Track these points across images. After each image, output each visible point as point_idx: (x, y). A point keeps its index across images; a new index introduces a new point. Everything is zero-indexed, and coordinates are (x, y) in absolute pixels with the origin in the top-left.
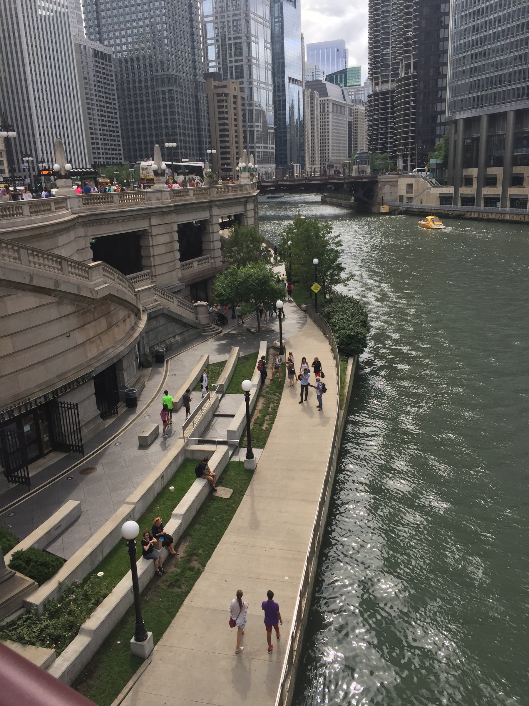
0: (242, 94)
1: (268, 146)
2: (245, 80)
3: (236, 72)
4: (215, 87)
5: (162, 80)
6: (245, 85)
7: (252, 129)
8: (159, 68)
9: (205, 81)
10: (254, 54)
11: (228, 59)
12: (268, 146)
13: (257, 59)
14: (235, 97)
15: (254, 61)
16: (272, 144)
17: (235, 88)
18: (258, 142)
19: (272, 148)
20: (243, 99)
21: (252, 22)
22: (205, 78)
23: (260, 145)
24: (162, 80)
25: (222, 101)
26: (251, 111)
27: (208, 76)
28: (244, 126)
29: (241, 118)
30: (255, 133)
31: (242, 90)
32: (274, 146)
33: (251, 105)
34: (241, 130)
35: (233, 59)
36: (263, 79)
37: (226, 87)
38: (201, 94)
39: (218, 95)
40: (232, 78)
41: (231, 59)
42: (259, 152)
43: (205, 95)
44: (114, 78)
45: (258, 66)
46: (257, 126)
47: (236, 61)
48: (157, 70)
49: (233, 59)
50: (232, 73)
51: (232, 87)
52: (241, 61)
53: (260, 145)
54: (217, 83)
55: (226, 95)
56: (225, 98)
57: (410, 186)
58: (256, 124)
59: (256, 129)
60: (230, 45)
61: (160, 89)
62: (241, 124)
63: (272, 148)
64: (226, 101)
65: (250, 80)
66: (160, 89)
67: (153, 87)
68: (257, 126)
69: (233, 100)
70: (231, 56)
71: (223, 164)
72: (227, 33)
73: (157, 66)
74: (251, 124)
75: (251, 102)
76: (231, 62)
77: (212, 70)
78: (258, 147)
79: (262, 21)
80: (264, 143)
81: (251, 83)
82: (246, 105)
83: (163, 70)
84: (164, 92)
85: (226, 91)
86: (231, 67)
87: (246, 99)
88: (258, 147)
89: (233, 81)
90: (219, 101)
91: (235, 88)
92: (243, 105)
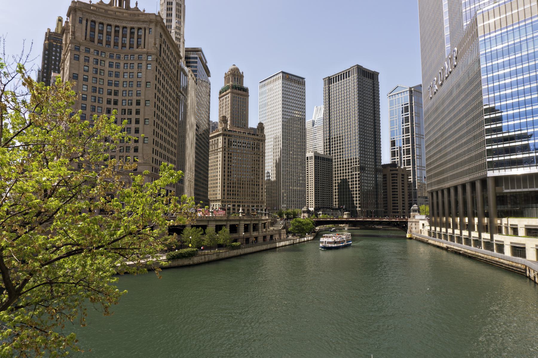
4: (391, 170)
5: (356, 169)
8: (355, 163)
11: (403, 157)
14: (403, 175)
24: (356, 169)
27: (385, 166)
35: (405, 156)
39: (392, 174)
55: (397, 174)
56: (396, 176)
57: (423, 225)
61: (354, 173)
66: (354, 173)
67: (351, 172)
69: (401, 176)
70: (404, 155)
71: (393, 209)
84: (356, 174)
90: (392, 177)
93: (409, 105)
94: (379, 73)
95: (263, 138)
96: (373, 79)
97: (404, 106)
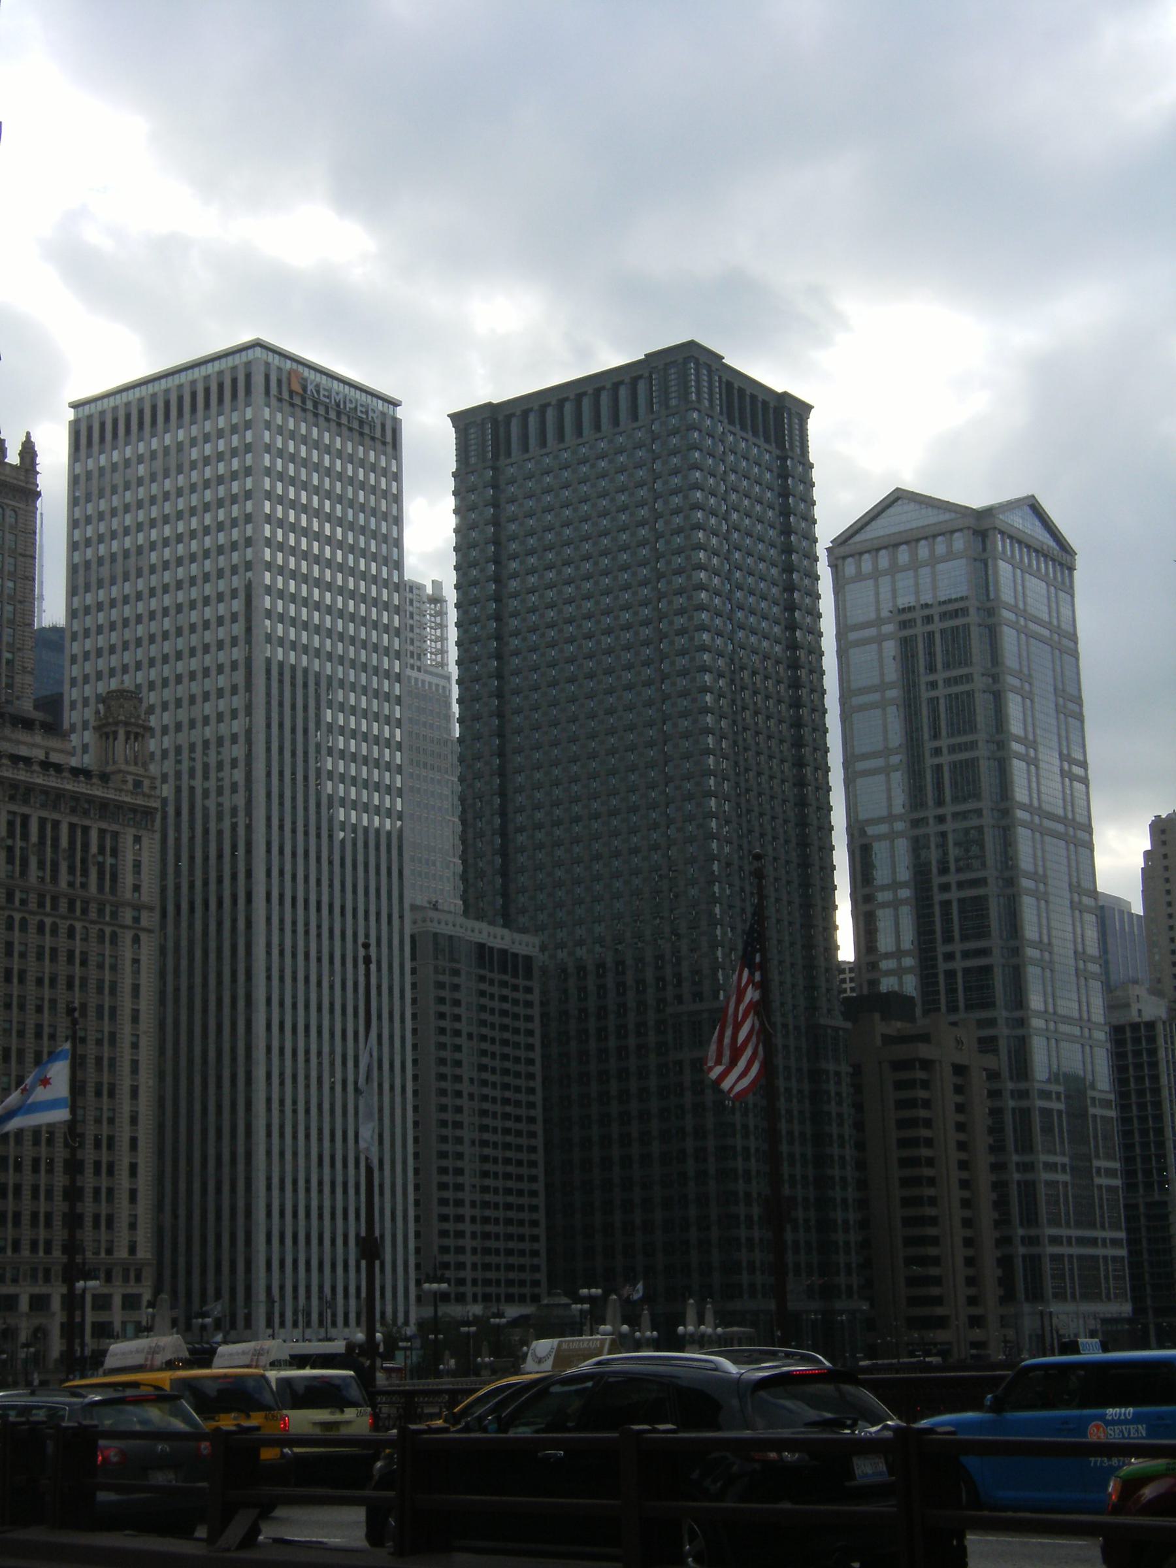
0: (990, 1061)
1: (1099, 1234)
2: (1002, 1013)
3: (965, 989)
4: (888, 1040)
6: (1003, 1031)
7: (1029, 1176)
9: (849, 1025)
10: (1030, 931)
12: (1099, 1234)
13: (1046, 946)
14: (960, 1070)
15: (1031, 953)
16: (1116, 1226)
17: (959, 1042)
18: (1055, 1222)
19: (1115, 1242)
20: (993, 1075)
21: (1023, 834)
22: (847, 1016)
23: (1064, 1232)
25: (911, 1084)
26: (1024, 1115)
28: (998, 1167)
29: (982, 1140)
30: (1042, 1191)
31: (988, 1045)
32: (1122, 1235)
33: (1023, 1094)
34: (984, 1179)
35: (957, 947)
36: (1068, 1006)
37: (925, 1038)
38: (831, 1067)
40: (953, 1008)
41: (949, 948)
42: (1056, 1258)
43: (845, 1068)
44: (536, 1026)
45: (1048, 966)
46: (1051, 1167)
47: (966, 955)
48: (679, 999)
49: (957, 947)
50: (955, 991)
51: (951, 1042)
52: (984, 952)
53: (1064, 1232)
54: (896, 1027)
55: (927, 1065)
56: (921, 1075)
58: (1043, 1158)
59: (1046, 1176)
60: (946, 904)
62: (983, 1159)
63: (1115, 1242)
64: (925, 1084)
65: (1017, 1014)
68: (1051, 1167)
72: (934, 870)
73: (679, 984)
74: (1027, 1158)
75: (1022, 1086)
76: (949, 957)
77: (887, 984)
78: (1055, 1240)
79: (1060, 828)
80: (1079, 1224)
81: (1022, 1022)
82: (1006, 1094)
83: (698, 996)
85: (924, 1051)
86: (951, 974)
87: (1005, 1073)
88: (1055, 1240)
89: (962, 1015)
91: (959, 1042)
92: (995, 1094)
93: (973, 618)
94: (808, 408)
95: (140, 801)
96: (780, 444)
97: (937, 626)
